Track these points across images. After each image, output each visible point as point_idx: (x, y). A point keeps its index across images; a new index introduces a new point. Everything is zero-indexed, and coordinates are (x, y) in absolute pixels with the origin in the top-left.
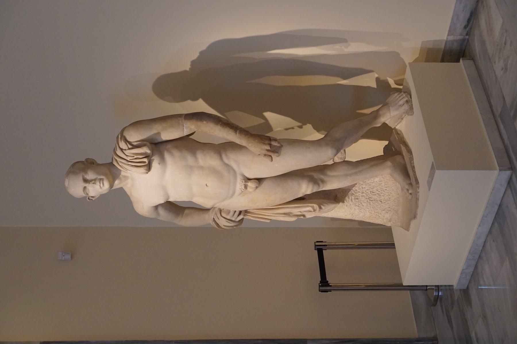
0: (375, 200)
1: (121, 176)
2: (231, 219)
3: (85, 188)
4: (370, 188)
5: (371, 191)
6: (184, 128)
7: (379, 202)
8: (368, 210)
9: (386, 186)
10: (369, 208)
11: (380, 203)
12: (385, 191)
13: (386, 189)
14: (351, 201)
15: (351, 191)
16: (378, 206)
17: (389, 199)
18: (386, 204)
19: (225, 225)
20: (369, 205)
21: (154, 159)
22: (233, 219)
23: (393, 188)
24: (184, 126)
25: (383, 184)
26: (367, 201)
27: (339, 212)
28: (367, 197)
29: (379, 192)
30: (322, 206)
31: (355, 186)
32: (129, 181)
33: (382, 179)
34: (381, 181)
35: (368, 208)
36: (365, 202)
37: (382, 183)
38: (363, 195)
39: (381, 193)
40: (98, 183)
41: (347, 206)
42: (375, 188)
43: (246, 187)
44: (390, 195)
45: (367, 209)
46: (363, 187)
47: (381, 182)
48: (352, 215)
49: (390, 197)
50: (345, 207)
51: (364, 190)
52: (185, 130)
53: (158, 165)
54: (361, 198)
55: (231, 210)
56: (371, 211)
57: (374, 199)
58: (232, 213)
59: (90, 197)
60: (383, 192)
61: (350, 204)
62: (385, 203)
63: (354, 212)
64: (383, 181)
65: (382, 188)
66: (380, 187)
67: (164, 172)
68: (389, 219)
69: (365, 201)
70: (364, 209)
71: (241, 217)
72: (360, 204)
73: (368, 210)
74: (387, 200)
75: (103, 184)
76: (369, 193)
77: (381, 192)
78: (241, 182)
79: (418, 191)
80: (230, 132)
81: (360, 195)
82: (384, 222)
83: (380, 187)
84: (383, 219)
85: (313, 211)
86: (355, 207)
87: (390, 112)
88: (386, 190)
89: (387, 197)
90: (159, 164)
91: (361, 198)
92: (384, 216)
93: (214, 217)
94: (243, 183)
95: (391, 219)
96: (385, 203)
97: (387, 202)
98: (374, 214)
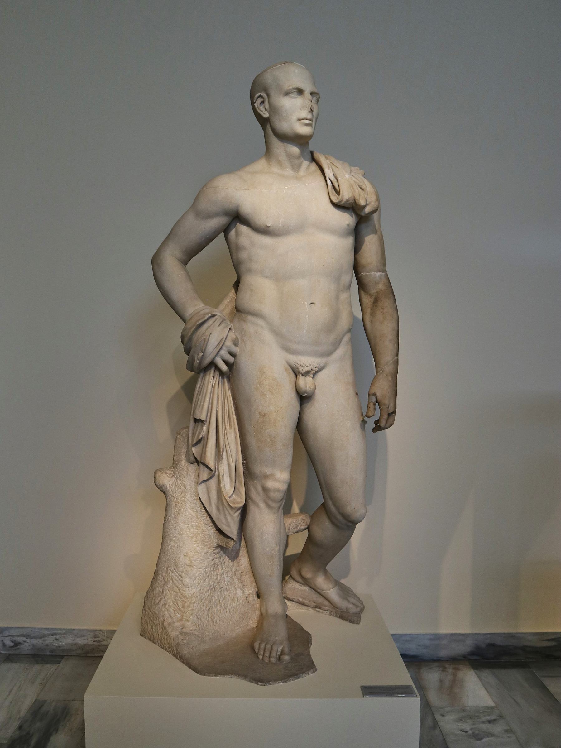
0: (211, 597)
1: (302, 159)
2: (224, 348)
3: (300, 92)
4: (228, 585)
5: (223, 587)
6: (381, 273)
7: (209, 606)
8: (197, 592)
9: (231, 610)
10: (201, 591)
11: (208, 608)
12: (225, 611)
13: (228, 612)
14: (213, 558)
15: (224, 555)
16: (203, 606)
17: (215, 621)
18: (208, 618)
19: (212, 336)
20: (205, 590)
21: (352, 217)
22: (224, 352)
23: (231, 623)
24: (383, 272)
25: (234, 604)
26: (211, 586)
27: (196, 541)
28: (215, 585)
29: (222, 602)
30: (239, 511)
31: (230, 559)
32: (289, 172)
33: (241, 601)
34: (238, 600)
35: (200, 590)
36: (209, 582)
37: (234, 602)
38: (219, 577)
39: (221, 606)
40: (309, 116)
41: (206, 553)
42: (227, 593)
43: (307, 373)
44: (220, 621)
45: (198, 590)
46: (228, 573)
47: (236, 600)
48: (188, 566)
49: (218, 621)
50: (205, 551)
51: (225, 575)
52: (378, 274)
53: (347, 222)
54: (215, 574)
55: (238, 348)
56: (197, 597)
57: (213, 596)
58: (235, 349)
59: (262, 100)
60: (223, 607)
61: (208, 558)
62: (209, 617)
63: (195, 567)
64: (238, 603)
65: (228, 604)
66: (229, 601)
67: (333, 232)
68: (184, 630)
69: (210, 582)
70: (199, 584)
71: (224, 368)
72: (208, 574)
73: (197, 592)
74: (212, 618)
75: (307, 125)
76: (221, 586)
77: (223, 605)
78: (315, 364)
79: (310, 673)
80: (395, 345)
81: (218, 570)
82: (174, 623)
83: (230, 601)
84: (181, 620)
85: (229, 496)
86: (204, 567)
87: (334, 587)
88: (226, 612)
89: (218, 617)
90: (348, 225)
91: (215, 574)
92: (188, 621)
93: (216, 317)
94: (315, 369)
95: (186, 634)
96: (209, 617)
97: (210, 619)
98: (191, 603)
